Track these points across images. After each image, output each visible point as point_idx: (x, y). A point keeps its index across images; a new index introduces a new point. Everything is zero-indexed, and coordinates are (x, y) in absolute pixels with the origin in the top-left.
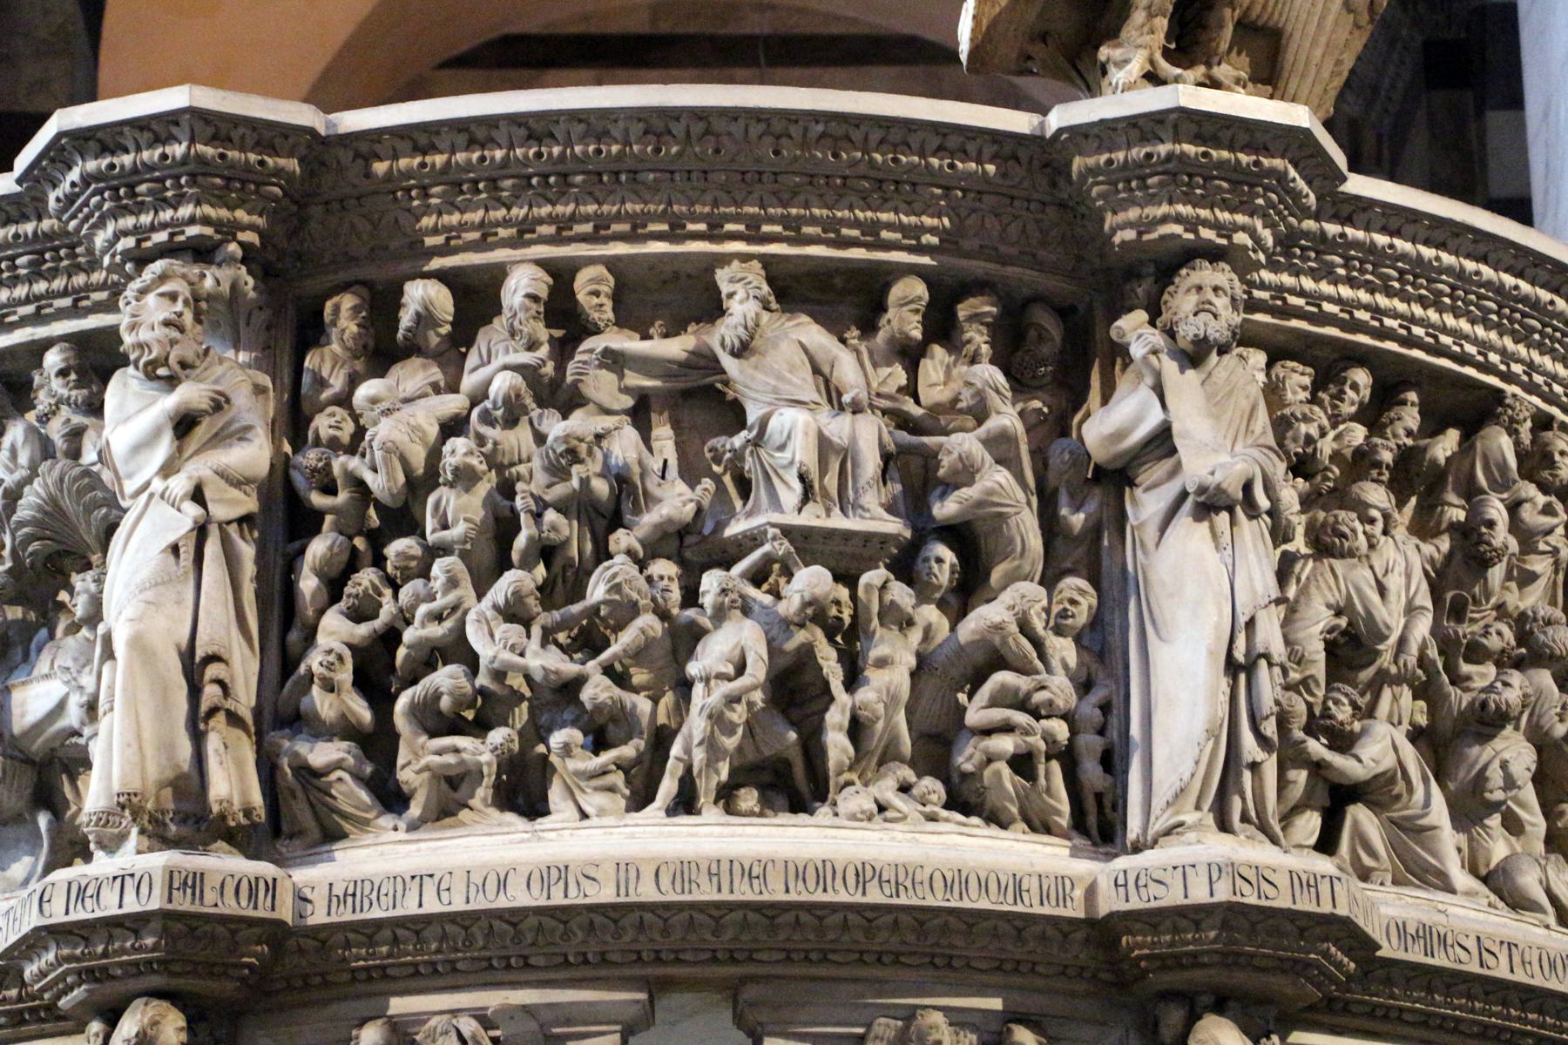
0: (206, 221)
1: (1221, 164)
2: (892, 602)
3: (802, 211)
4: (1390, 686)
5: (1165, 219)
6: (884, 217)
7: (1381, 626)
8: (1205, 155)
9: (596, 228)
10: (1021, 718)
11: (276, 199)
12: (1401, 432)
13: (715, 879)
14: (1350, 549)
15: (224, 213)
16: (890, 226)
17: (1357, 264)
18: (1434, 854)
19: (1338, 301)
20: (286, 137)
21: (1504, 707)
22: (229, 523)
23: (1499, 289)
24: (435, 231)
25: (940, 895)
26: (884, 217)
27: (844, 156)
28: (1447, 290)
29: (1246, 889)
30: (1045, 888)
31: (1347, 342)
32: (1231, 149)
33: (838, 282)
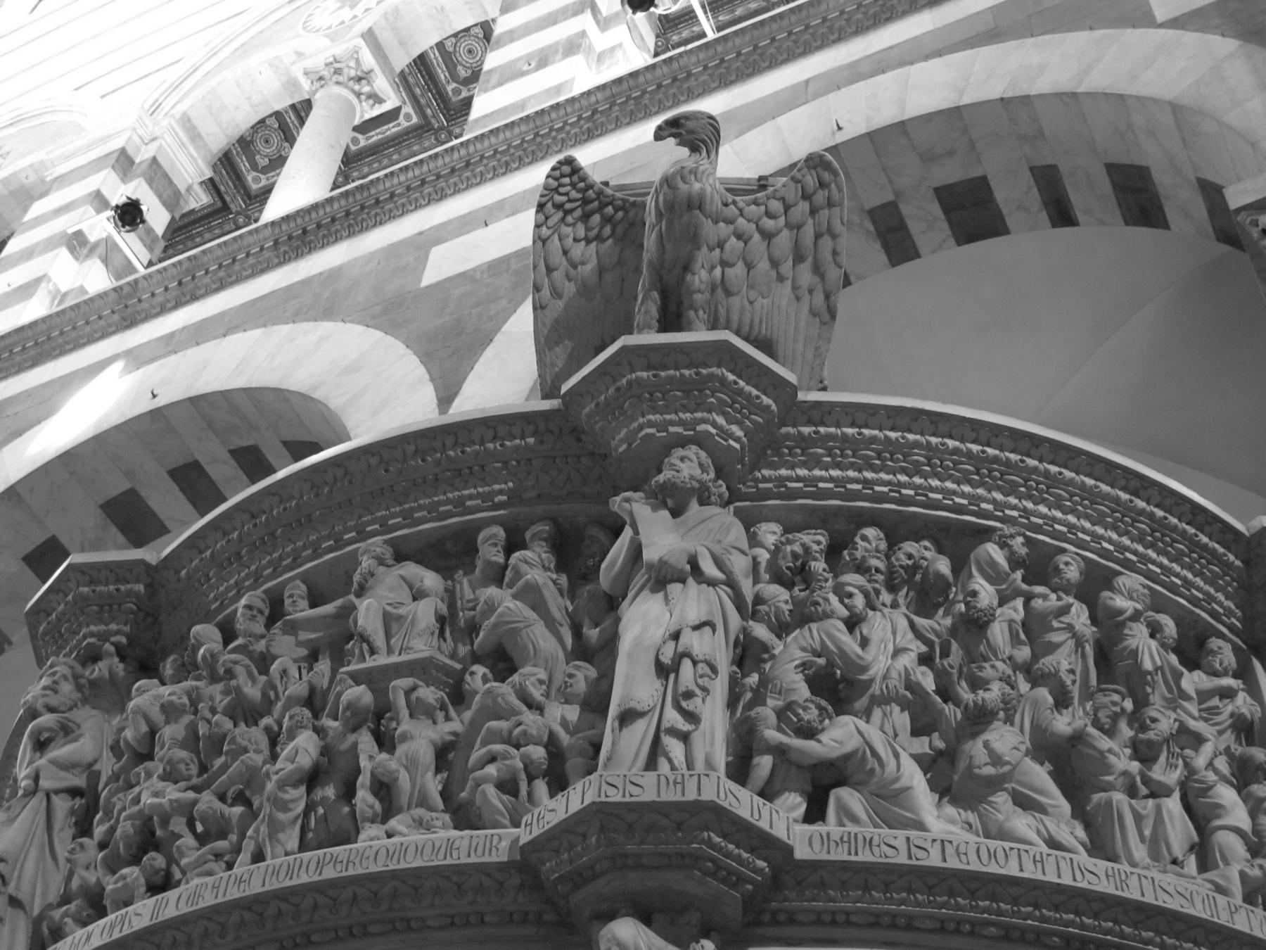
0: (92, 634)
1: (670, 379)
2: (417, 698)
4: (879, 706)
5: (641, 428)
6: (466, 492)
7: (854, 657)
9: (295, 560)
10: (498, 748)
11: (132, 612)
12: (902, 556)
13: (215, 890)
15: (102, 628)
16: (471, 497)
17: (838, 452)
18: (909, 810)
19: (831, 479)
20: (131, 571)
21: (980, 703)
22: (57, 792)
26: (466, 492)
27: (429, 458)
28: (922, 459)
29: (611, 791)
30: (474, 844)
31: (849, 507)
32: (676, 368)
33: (449, 546)
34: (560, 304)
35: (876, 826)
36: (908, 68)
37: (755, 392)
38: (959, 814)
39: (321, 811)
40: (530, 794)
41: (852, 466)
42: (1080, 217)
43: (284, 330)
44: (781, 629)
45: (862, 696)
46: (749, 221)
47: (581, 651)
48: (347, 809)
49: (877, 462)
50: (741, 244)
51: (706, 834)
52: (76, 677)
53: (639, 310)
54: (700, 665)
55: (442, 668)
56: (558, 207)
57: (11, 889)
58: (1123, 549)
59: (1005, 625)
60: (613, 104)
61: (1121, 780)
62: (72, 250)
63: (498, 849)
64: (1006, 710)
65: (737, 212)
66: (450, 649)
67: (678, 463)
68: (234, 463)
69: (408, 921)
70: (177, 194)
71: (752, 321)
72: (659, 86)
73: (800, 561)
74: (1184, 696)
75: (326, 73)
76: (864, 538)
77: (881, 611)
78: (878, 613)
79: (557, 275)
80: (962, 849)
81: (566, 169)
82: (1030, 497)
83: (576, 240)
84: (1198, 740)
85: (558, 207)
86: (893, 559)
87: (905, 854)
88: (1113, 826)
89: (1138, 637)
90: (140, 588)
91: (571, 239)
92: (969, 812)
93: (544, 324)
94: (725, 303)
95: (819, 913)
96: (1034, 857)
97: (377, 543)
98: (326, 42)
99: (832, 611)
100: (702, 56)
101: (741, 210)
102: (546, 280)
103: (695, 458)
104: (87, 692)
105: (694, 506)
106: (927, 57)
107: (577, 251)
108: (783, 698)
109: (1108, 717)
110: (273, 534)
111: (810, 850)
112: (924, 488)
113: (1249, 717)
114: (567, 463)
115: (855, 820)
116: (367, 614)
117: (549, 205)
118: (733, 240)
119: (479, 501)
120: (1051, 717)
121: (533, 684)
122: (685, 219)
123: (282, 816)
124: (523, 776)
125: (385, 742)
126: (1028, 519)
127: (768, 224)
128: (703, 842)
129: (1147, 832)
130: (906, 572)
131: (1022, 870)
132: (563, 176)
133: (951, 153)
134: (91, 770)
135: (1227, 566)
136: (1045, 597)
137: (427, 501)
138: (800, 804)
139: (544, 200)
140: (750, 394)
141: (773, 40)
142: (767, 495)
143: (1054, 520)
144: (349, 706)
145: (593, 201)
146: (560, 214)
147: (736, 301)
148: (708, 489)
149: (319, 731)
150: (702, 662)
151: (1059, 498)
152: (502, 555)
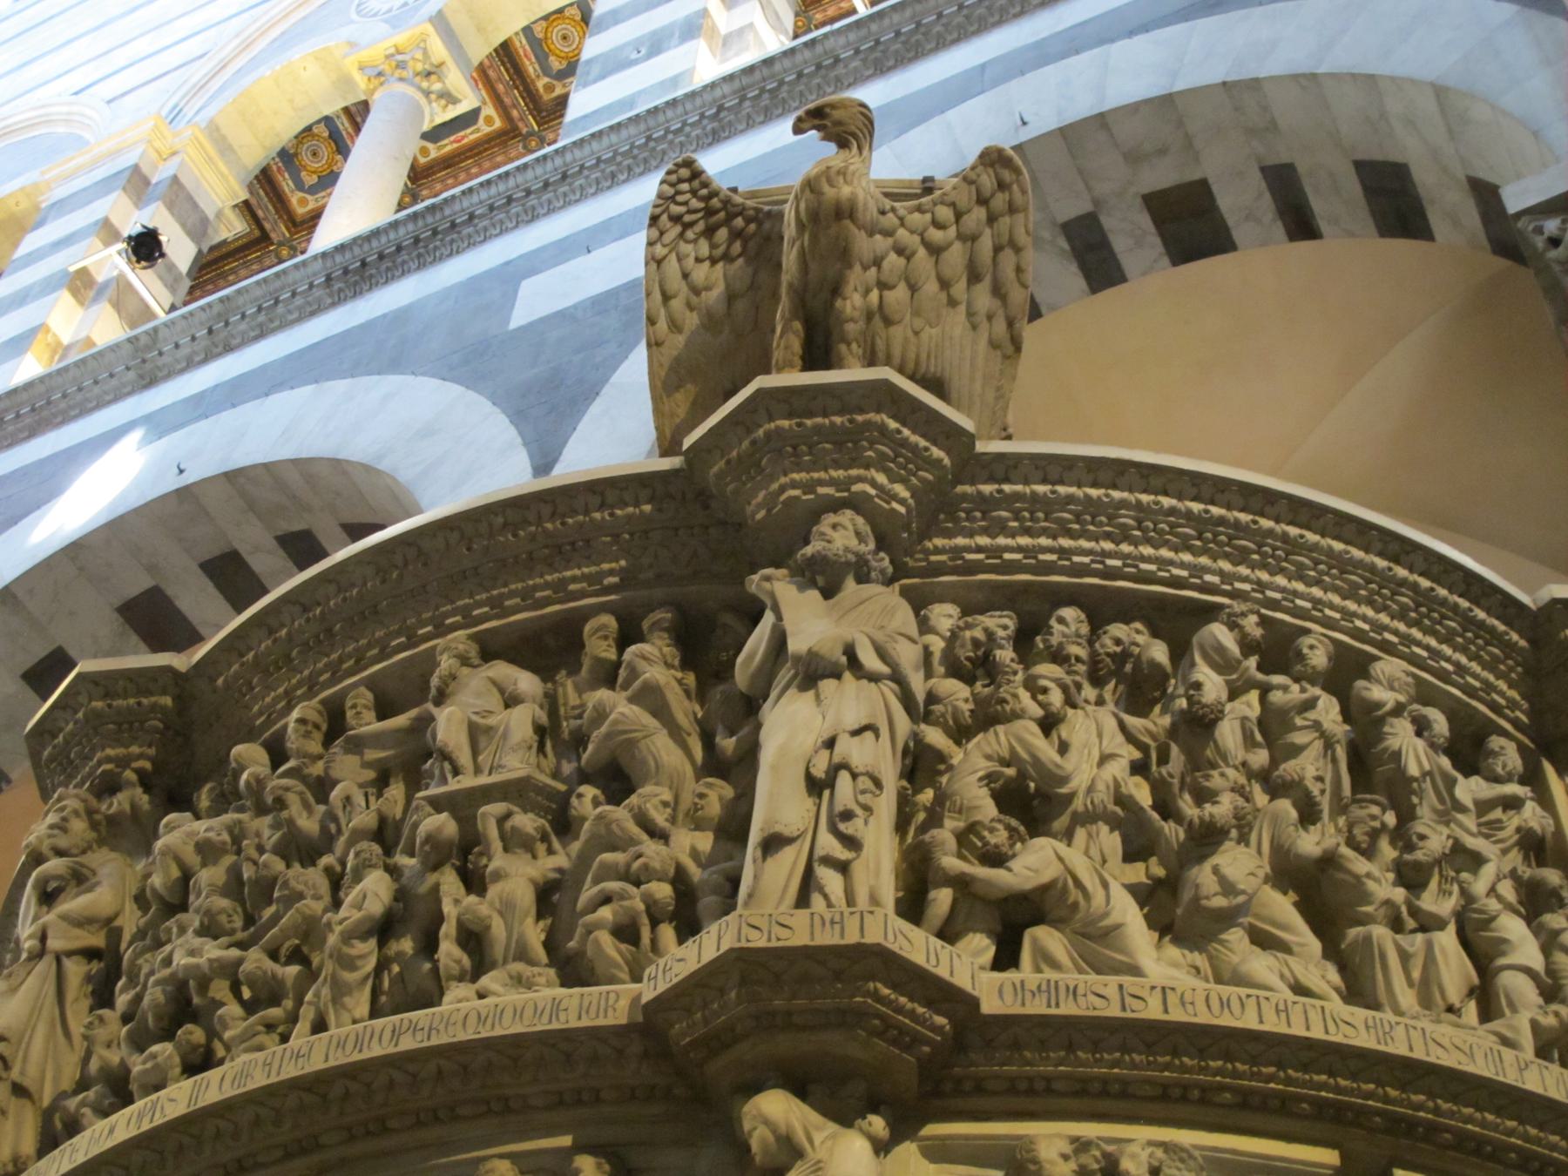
0: (109, 760)
1: (818, 429)
2: (513, 828)
3: (503, 590)
4: (1083, 825)
5: (783, 489)
6: (568, 574)
7: (1051, 767)
8: (799, 425)
9: (357, 662)
10: (613, 886)
11: (156, 730)
13: (267, 1068)
14: (1013, 711)
15: (120, 751)
16: (574, 579)
18: (1122, 951)
19: (1019, 549)
22: (70, 954)
23: (1189, 515)
24: (261, 713)
25: (470, 1031)
26: (568, 574)
27: (522, 533)
29: (754, 934)
30: (586, 1004)
32: (825, 415)
34: (680, 340)
35: (1081, 971)
36: (1105, 47)
37: (923, 443)
38: (1184, 956)
39: (396, 969)
40: (654, 942)
41: (1044, 532)
42: (1323, 226)
43: (340, 386)
44: (961, 733)
45: (1060, 814)
46: (912, 232)
47: (714, 766)
48: (427, 966)
49: (1076, 526)
50: (902, 261)
51: (871, 985)
52: (90, 813)
53: (778, 345)
54: (861, 779)
55: (542, 790)
56: (675, 219)
57: (15, 1074)
58: (1379, 628)
59: (1237, 724)
60: (743, 99)
61: (1382, 911)
62: (75, 293)
63: (615, 1010)
64: (1239, 827)
65: (896, 221)
66: (552, 766)
67: (828, 531)
68: (281, 552)
69: (507, 1099)
70: (204, 221)
71: (918, 356)
72: (800, 75)
73: (983, 650)
74: (1460, 807)
75: (386, 68)
76: (1061, 621)
77: (1083, 708)
78: (1080, 712)
79: (677, 304)
80: (1188, 998)
81: (685, 172)
82: (1264, 566)
83: (698, 260)
84: (1476, 861)
85: (675, 219)
86: (1097, 645)
87: (1118, 1005)
88: (1373, 968)
89: (1400, 735)
90: (167, 701)
91: (691, 260)
92: (1196, 954)
93: (661, 365)
94: (884, 336)
95: (1012, 1080)
96: (1277, 1005)
97: (459, 639)
98: (384, 28)
99: (1023, 710)
100: (852, 36)
101: (901, 219)
102: (662, 312)
103: (851, 527)
104: (103, 830)
105: (850, 584)
106: (1131, 33)
107: (701, 273)
108: (964, 817)
109: (1366, 834)
110: (329, 631)
111: (1000, 1003)
112: (1135, 558)
113: (1539, 830)
114: (693, 535)
115: (1055, 965)
116: (449, 726)
117: (664, 217)
118: (893, 256)
119: (584, 585)
120: (1294, 834)
121: (656, 808)
122: (833, 231)
123: (350, 977)
124: (645, 920)
125: (474, 882)
126: (1263, 593)
127: (936, 235)
128: (867, 994)
129: (1416, 974)
130: (1113, 661)
131: (1261, 1022)
132: (681, 181)
133: (1162, 152)
134: (109, 925)
135: (1508, 647)
136: (1285, 689)
137: (520, 585)
138: (987, 948)
139: (658, 211)
140: (917, 445)
141: (940, 15)
142: (939, 570)
143: (1296, 594)
144: (429, 839)
145: (716, 212)
146: (678, 229)
147: (897, 332)
148: (866, 562)
149: (393, 871)
150: (863, 774)
151: (1301, 566)
152: (614, 650)
